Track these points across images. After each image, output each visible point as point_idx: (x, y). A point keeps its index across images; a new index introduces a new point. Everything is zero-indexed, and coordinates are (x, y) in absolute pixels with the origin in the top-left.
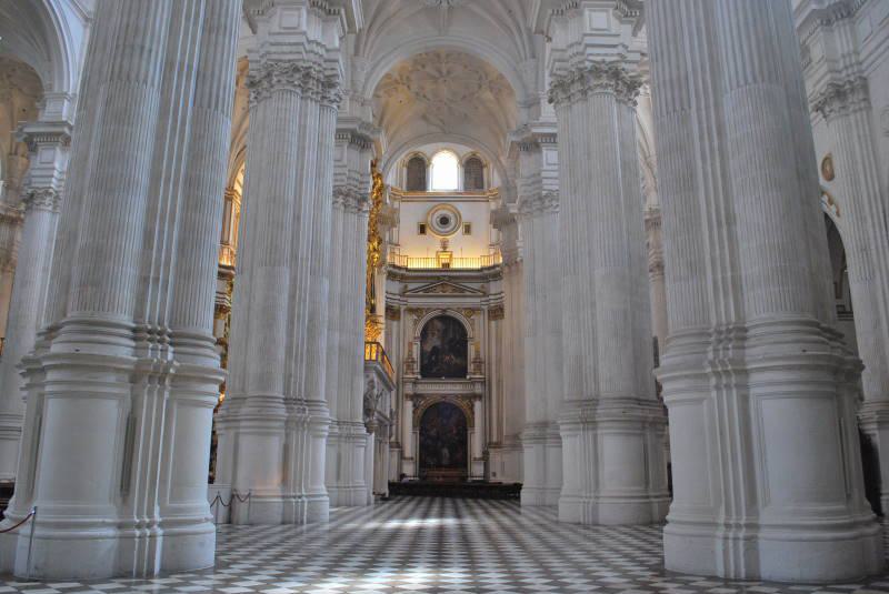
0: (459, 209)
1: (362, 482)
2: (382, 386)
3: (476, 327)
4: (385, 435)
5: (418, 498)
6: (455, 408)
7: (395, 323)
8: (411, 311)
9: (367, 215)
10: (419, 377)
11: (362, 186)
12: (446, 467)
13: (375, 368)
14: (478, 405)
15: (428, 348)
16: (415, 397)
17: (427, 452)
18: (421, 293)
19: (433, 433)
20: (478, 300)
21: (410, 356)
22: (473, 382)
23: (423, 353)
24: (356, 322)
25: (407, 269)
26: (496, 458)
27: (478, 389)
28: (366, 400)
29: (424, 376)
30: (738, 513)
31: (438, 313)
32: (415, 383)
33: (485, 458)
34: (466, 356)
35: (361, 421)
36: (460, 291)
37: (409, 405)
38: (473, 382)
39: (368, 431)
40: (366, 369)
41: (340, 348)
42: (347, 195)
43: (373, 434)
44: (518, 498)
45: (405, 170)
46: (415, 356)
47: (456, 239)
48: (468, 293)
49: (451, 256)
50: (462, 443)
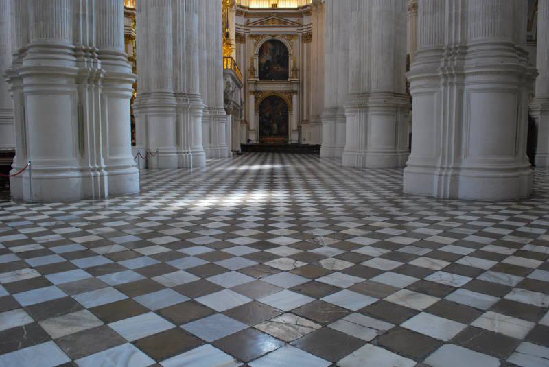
1: (224, 144)
2: (235, 85)
3: (294, 47)
5: (259, 153)
6: (280, 99)
7: (242, 45)
8: (252, 36)
10: (258, 80)
12: (276, 135)
13: (231, 74)
14: (295, 97)
15: (264, 61)
16: (256, 92)
17: (264, 127)
18: (258, 25)
19: (267, 114)
20: (295, 29)
21: (252, 66)
22: (292, 83)
23: (260, 63)
24: (216, 43)
25: (249, 8)
26: (306, 130)
27: (295, 87)
28: (225, 94)
29: (261, 79)
30: (449, 161)
31: (270, 38)
32: (256, 83)
33: (299, 129)
35: (222, 107)
36: (284, 23)
37: (252, 97)
38: (292, 83)
40: (224, 74)
41: (208, 61)
43: (231, 115)
44: (319, 153)
46: (255, 66)
48: (289, 25)
50: (285, 121)
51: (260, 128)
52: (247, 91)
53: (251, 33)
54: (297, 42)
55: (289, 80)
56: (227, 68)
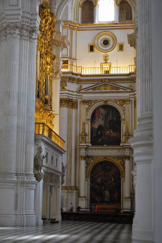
0: (116, 35)
1: (32, 211)
3: (127, 112)
4: (56, 181)
6: (112, 165)
7: (74, 110)
8: (84, 102)
9: (36, 41)
10: (90, 145)
11: (33, 22)
12: (107, 202)
13: (43, 140)
14: (127, 162)
15: (96, 126)
16: (87, 158)
18: (91, 91)
19: (99, 181)
20: (128, 94)
21: (84, 131)
22: (124, 148)
23: (92, 130)
24: (28, 110)
25: (81, 75)
28: (35, 160)
31: (102, 103)
34: (120, 131)
35: (32, 173)
36: (116, 89)
37: (83, 163)
38: (124, 148)
39: (36, 180)
40: (36, 140)
41: (18, 127)
42: (22, 28)
43: (42, 181)
45: (80, 9)
46: (87, 131)
47: (114, 54)
48: (121, 90)
49: (110, 66)
51: (91, 195)
52: (78, 157)
53: (86, 99)
54: (128, 107)
55: (121, 145)
56: (39, 134)
